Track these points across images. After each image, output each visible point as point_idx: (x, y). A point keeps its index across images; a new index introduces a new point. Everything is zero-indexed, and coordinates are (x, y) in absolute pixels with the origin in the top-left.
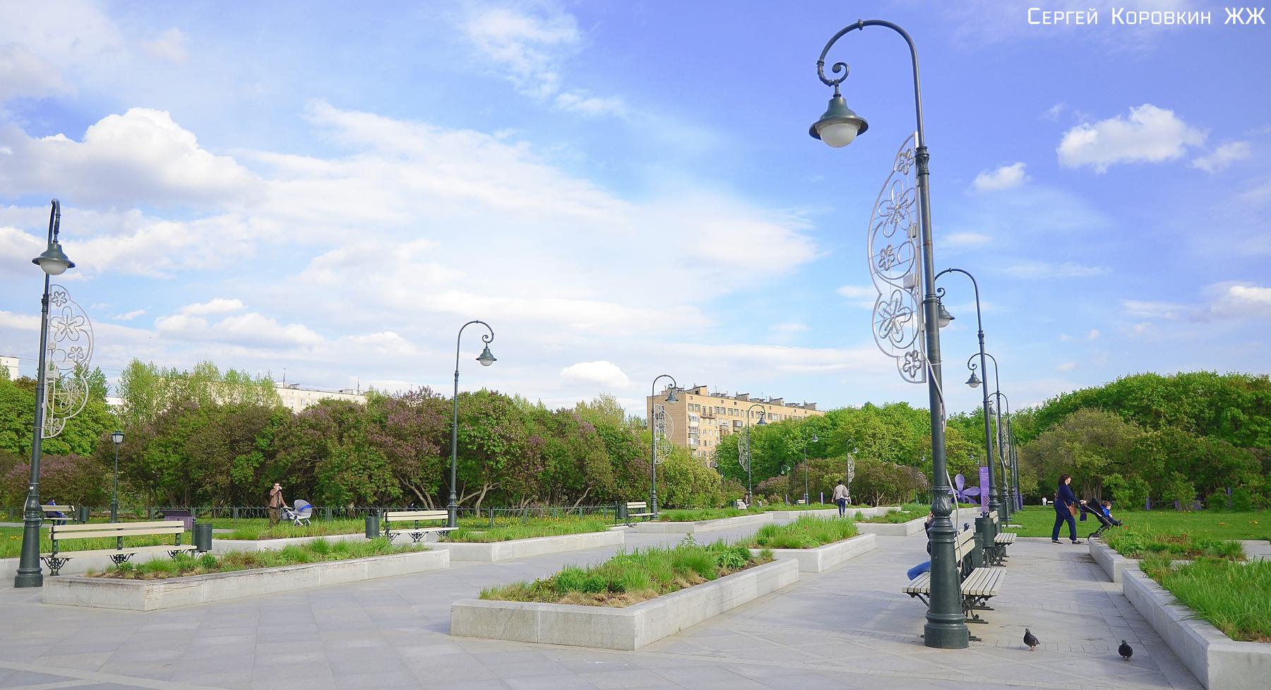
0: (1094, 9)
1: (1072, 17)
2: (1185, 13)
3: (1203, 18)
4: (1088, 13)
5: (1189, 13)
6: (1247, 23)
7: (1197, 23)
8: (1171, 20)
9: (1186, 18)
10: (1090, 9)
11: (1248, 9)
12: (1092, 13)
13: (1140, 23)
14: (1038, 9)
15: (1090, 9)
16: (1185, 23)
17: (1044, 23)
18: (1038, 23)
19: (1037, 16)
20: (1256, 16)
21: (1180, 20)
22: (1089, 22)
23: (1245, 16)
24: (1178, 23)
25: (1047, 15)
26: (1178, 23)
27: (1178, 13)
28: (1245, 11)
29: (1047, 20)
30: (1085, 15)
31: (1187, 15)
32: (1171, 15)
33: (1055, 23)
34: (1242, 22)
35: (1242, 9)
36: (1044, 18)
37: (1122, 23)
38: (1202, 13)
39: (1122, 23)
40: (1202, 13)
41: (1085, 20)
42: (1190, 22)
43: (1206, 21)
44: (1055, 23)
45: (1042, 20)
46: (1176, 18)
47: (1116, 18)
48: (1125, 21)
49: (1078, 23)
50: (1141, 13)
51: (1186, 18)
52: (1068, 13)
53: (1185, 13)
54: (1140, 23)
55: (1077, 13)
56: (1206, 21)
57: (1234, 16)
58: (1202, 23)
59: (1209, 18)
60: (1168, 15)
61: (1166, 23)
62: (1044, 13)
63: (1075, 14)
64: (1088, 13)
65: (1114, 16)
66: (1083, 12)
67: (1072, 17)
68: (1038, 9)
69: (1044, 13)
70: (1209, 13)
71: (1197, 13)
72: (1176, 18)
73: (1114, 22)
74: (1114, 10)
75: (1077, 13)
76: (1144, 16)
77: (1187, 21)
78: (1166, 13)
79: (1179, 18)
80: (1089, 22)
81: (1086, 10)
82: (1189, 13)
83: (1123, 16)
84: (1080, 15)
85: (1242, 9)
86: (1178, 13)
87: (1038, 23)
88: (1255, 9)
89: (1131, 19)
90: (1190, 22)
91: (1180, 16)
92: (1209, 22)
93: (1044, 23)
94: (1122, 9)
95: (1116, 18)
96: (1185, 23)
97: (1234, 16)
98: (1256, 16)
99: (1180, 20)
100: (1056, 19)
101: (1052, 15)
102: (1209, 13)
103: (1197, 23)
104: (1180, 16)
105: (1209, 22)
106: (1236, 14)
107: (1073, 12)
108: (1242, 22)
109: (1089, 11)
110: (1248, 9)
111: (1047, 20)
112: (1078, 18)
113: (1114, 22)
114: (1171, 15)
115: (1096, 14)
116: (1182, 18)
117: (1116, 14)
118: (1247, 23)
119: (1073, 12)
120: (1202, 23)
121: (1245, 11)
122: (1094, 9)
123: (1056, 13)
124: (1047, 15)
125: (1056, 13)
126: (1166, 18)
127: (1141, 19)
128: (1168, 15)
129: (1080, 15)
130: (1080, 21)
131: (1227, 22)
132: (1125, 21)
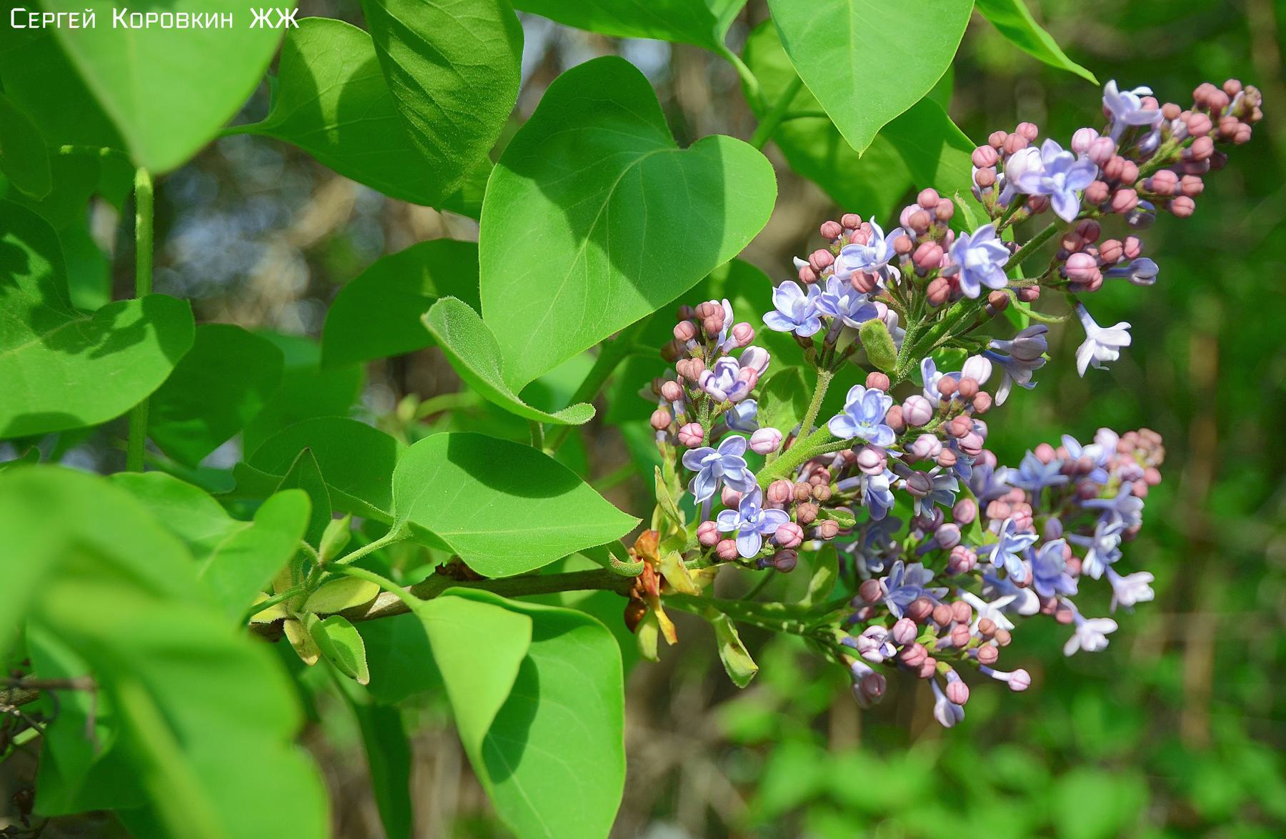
0: (91, 10)
2: (201, 14)
3: (223, 20)
4: (84, 14)
5: (207, 14)
7: (216, 26)
8: (184, 23)
9: (203, 20)
10: (87, 10)
11: (278, 10)
12: (88, 15)
13: (147, 27)
14: (23, 10)
15: (87, 10)
16: (202, 27)
17: (31, 26)
18: (23, 27)
19: (21, 18)
21: (196, 23)
22: (85, 26)
24: (193, 26)
25: (33, 17)
26: (193, 26)
27: (194, 15)
28: (274, 12)
29: (34, 24)
30: (80, 17)
32: (185, 17)
33: (44, 27)
34: (271, 26)
35: (271, 10)
36: (31, 20)
38: (223, 14)
39: (125, 26)
40: (223, 14)
41: (80, 23)
42: (208, 25)
43: (227, 24)
44: (44, 27)
45: (28, 25)
47: (118, 21)
49: (71, 27)
51: (203, 20)
52: (59, 14)
53: (201, 14)
54: (147, 27)
55: (71, 14)
56: (227, 24)
57: (262, 18)
58: (223, 26)
59: (231, 20)
60: (181, 17)
61: (178, 27)
62: (31, 14)
63: (68, 15)
64: (84, 14)
65: (115, 18)
66: (77, 14)
67: (65, 20)
68: (23, 10)
69: (31, 14)
70: (231, 14)
73: (115, 26)
74: (115, 10)
75: (71, 14)
77: (204, 24)
79: (194, 20)
80: (85, 26)
81: (82, 11)
82: (207, 14)
83: (126, 17)
84: (74, 17)
85: (271, 10)
86: (194, 15)
87: (23, 27)
90: (208, 25)
91: (196, 18)
92: (231, 26)
93: (31, 26)
94: (125, 10)
95: (118, 21)
96: (202, 27)
99: (196, 23)
100: (45, 22)
102: (231, 14)
103: (216, 26)
104: (196, 18)
105: (231, 26)
106: (264, 15)
107: (65, 14)
108: (271, 26)
109: (86, 12)
110: (278, 10)
111: (34, 24)
112: (71, 20)
113: (115, 26)
114: (185, 17)
115: (93, 15)
116: (198, 20)
117: (118, 15)
118: (277, 26)
119: (65, 14)
120: (223, 26)
121: (274, 12)
122: (91, 10)
123: (44, 14)
124: (33, 17)
126: (178, 20)
128: (181, 17)
129: (74, 17)
130: (74, 23)
131: (252, 26)
132: (128, 24)
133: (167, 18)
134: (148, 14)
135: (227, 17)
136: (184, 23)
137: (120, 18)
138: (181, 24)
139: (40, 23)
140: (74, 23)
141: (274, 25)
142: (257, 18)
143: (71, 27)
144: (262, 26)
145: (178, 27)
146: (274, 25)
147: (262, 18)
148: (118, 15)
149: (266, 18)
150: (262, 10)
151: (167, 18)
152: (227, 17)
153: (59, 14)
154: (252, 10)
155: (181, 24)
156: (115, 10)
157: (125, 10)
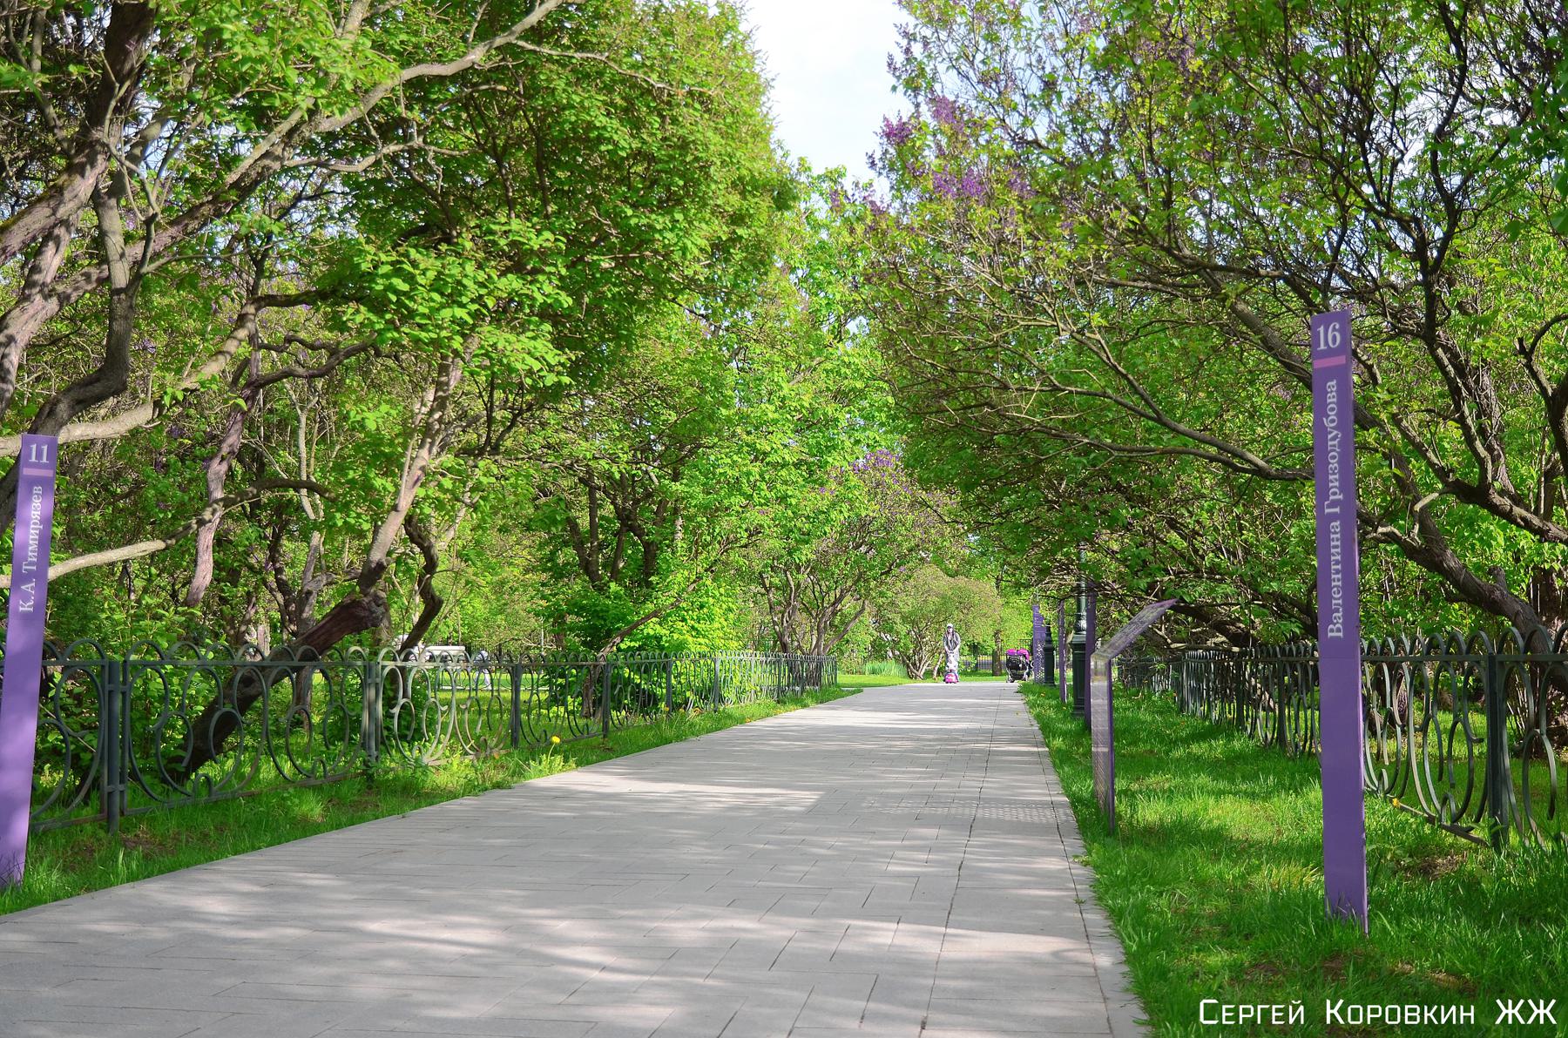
1: (1266, 1014)
3: (1462, 1014)
6: (1530, 1022)
8: (1414, 1019)
11: (1530, 1002)
12: (1295, 1008)
14: (1215, 1001)
17: (1224, 1022)
18: (1215, 1022)
19: (1212, 1012)
20: (1542, 1011)
21: (1429, 1018)
22: (1291, 1021)
23: (1526, 1012)
25: (1228, 1010)
29: (1228, 1018)
30: (1286, 1011)
31: (1438, 1011)
32: (1415, 1010)
34: (1522, 1022)
35: (1522, 1001)
36: (1224, 1014)
37: (1341, 1022)
39: (1341, 1022)
41: (1286, 1017)
43: (1467, 1019)
45: (1221, 1020)
46: (1422, 1014)
47: (1332, 1015)
48: (1344, 1018)
50: (1369, 1007)
51: (1437, 1015)
52: (1259, 1007)
56: (1467, 1019)
59: (1472, 1014)
60: (1410, 1010)
61: (1407, 1022)
62: (1224, 1007)
65: (1329, 1012)
67: (1266, 1014)
68: (1215, 1001)
69: (1224, 1007)
71: (1453, 1008)
72: (1422, 1014)
73: (1328, 1022)
74: (1328, 1002)
75: (1274, 1007)
76: (1374, 1011)
77: (1439, 1020)
78: (1407, 1007)
79: (1426, 1015)
80: (1291, 1021)
81: (1286, 1002)
83: (1342, 1011)
85: (1522, 1001)
87: (1215, 1022)
88: (1542, 1002)
89: (1355, 1017)
93: (1224, 1022)
94: (1341, 1001)
95: (1332, 1015)
97: (1509, 1011)
98: (1542, 1011)
99: (1429, 1018)
100: (1241, 1016)
101: (1236, 1011)
108: (1522, 1022)
110: (1530, 1002)
111: (1228, 1018)
112: (1274, 1014)
113: (1328, 1022)
114: (1415, 1010)
115: (1301, 1008)
116: (1431, 1014)
117: (1332, 1008)
118: (1530, 1022)
123: (1241, 1007)
124: (1228, 1010)
125: (1241, 1007)
126: (1407, 1014)
127: (1369, 1016)
128: (1410, 1010)
130: (1278, 1019)
132: (1344, 1018)
133: (1393, 1012)
134: (1369, 1007)
135: (1467, 1010)
136: (1414, 1019)
138: (1410, 1018)
139: (1236, 1017)
140: (1278, 1019)
141: (1526, 1020)
142: (1505, 1011)
143: (1274, 1022)
145: (1407, 1022)
146: (1526, 1020)
148: (1332, 1008)
149: (1516, 1011)
150: (1510, 1002)
152: (1467, 1010)
153: (1259, 1007)
154: (1498, 1001)
155: (1410, 1018)
156: (1328, 1002)
157: (1341, 1001)
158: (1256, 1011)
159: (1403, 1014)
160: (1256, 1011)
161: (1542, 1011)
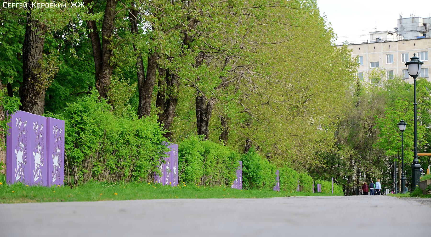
9: (57, 5)
17: (9, 7)
19: (6, 5)
25: (9, 4)
34: (77, 7)
36: (9, 5)
47: (33, 5)
51: (57, 5)
52: (17, 4)
55: (20, 4)
59: (65, 5)
61: (50, 7)
62: (9, 4)
65: (33, 5)
67: (18, 5)
74: (32, 3)
75: (20, 4)
77: (58, 7)
79: (55, 5)
80: (24, 7)
83: (36, 5)
87: (7, 7)
93: (9, 7)
95: (33, 5)
100: (13, 6)
111: (9, 6)
112: (20, 5)
115: (26, 4)
123: (13, 4)
126: (50, 5)
127: (42, 6)
134: (42, 4)
136: (52, 6)
137: (34, 5)
138: (51, 6)
139: (11, 6)
143: (20, 7)
144: (74, 7)
147: (74, 5)
151: (47, 6)
153: (17, 4)
158: (45, 5)
159: (49, 5)
160: (45, 5)
161: (81, 5)
